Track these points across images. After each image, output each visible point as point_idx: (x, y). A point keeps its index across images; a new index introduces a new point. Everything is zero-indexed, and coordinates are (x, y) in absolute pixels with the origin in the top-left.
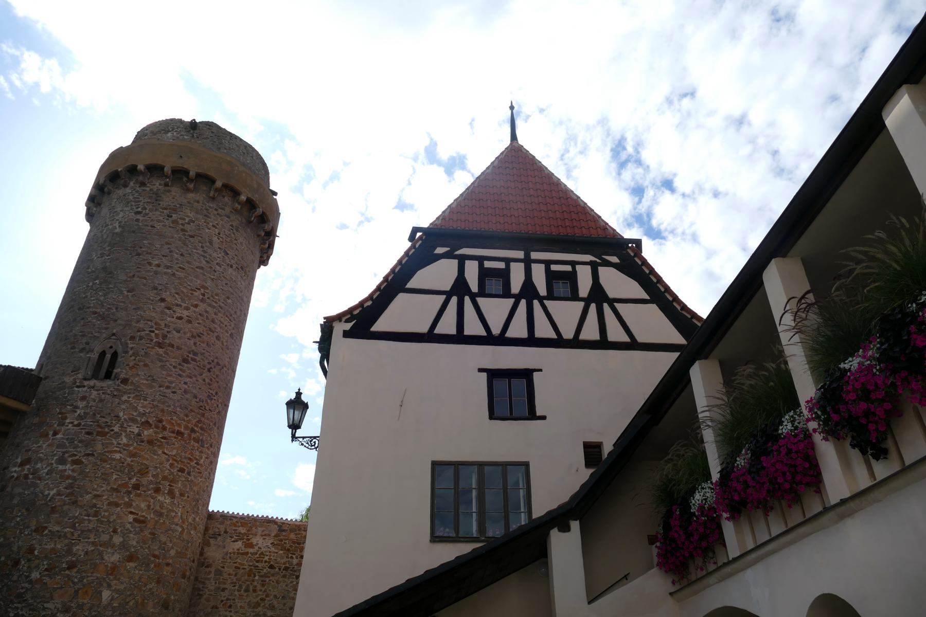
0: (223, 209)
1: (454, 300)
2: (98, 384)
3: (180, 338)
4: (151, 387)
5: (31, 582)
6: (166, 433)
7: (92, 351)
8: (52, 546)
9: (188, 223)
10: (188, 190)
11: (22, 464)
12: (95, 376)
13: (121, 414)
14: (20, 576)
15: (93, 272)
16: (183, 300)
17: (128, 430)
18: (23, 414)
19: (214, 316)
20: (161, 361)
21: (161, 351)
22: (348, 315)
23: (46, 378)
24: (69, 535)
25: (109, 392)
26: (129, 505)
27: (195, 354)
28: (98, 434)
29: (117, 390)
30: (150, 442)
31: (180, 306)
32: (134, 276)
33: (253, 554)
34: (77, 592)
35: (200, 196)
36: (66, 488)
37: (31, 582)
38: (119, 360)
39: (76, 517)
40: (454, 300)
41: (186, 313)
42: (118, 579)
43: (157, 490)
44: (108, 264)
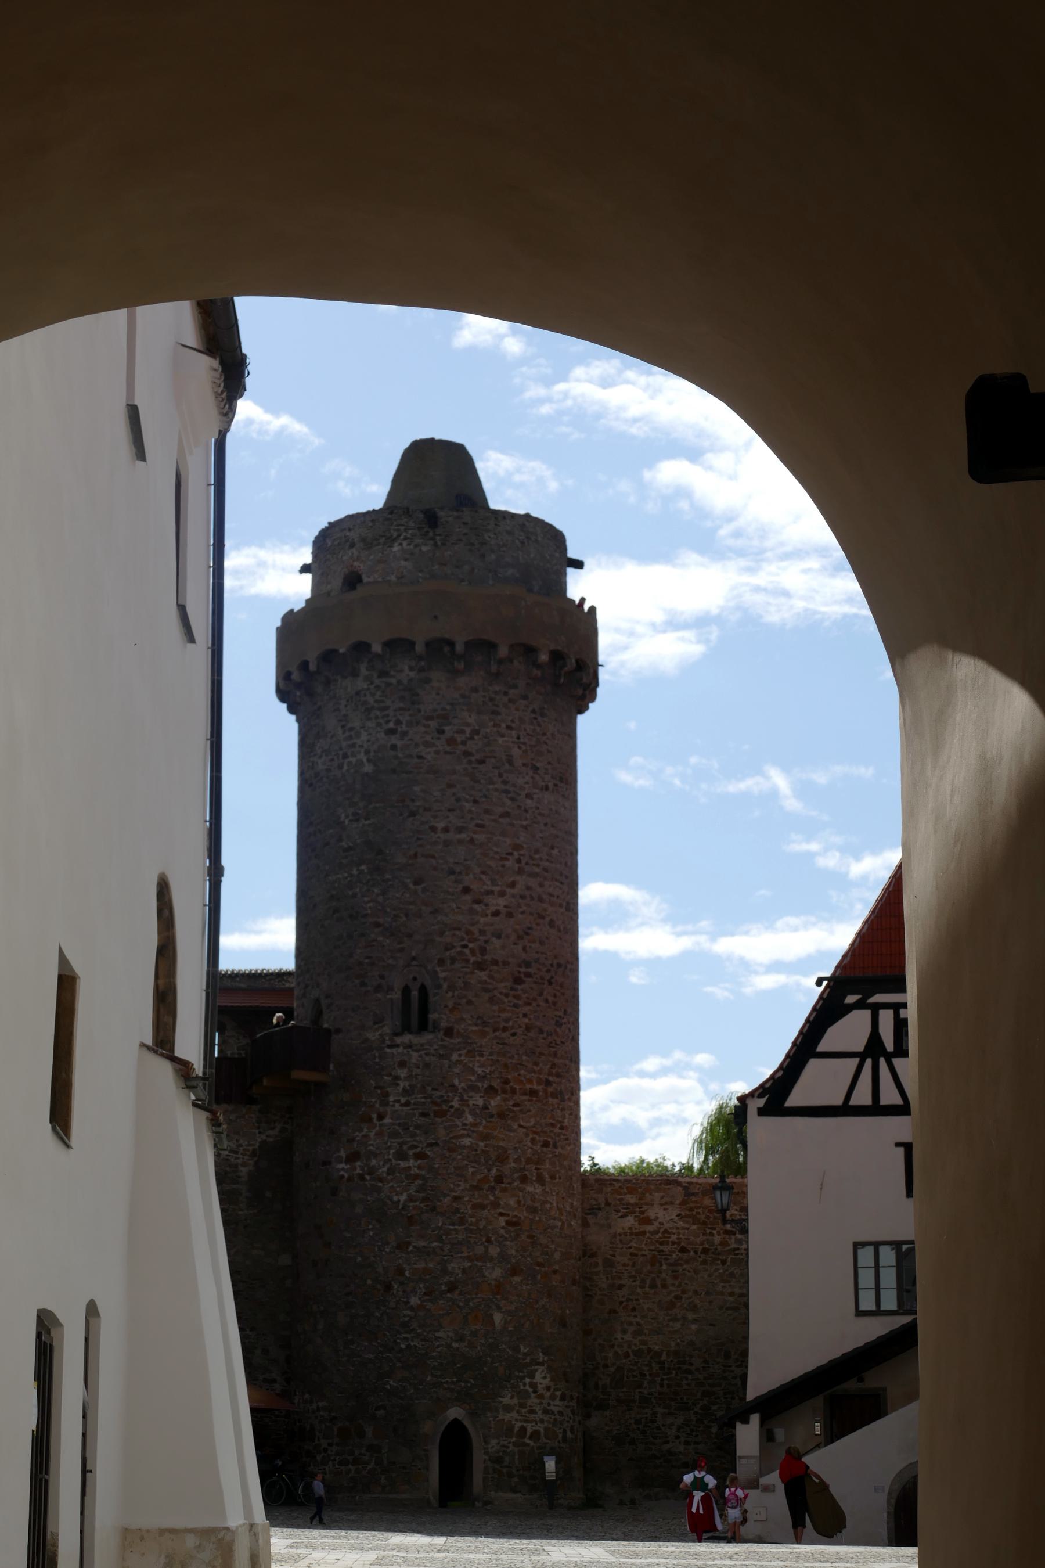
0: (515, 687)
1: (869, 1062)
2: (416, 1040)
3: (503, 947)
4: (483, 1034)
5: (412, 1308)
6: (518, 1098)
7: (390, 989)
8: (423, 1265)
9: (471, 738)
12: (406, 1028)
13: (456, 1082)
15: (350, 849)
16: (494, 882)
17: (471, 1103)
20: (486, 990)
21: (483, 975)
22: (762, 1090)
23: (338, 1031)
25: (432, 1051)
26: (496, 1205)
27: (528, 965)
28: (437, 1114)
30: (501, 1115)
31: (492, 892)
32: (416, 855)
36: (417, 1191)
38: (432, 999)
40: (869, 1062)
41: (502, 902)
43: (524, 1179)
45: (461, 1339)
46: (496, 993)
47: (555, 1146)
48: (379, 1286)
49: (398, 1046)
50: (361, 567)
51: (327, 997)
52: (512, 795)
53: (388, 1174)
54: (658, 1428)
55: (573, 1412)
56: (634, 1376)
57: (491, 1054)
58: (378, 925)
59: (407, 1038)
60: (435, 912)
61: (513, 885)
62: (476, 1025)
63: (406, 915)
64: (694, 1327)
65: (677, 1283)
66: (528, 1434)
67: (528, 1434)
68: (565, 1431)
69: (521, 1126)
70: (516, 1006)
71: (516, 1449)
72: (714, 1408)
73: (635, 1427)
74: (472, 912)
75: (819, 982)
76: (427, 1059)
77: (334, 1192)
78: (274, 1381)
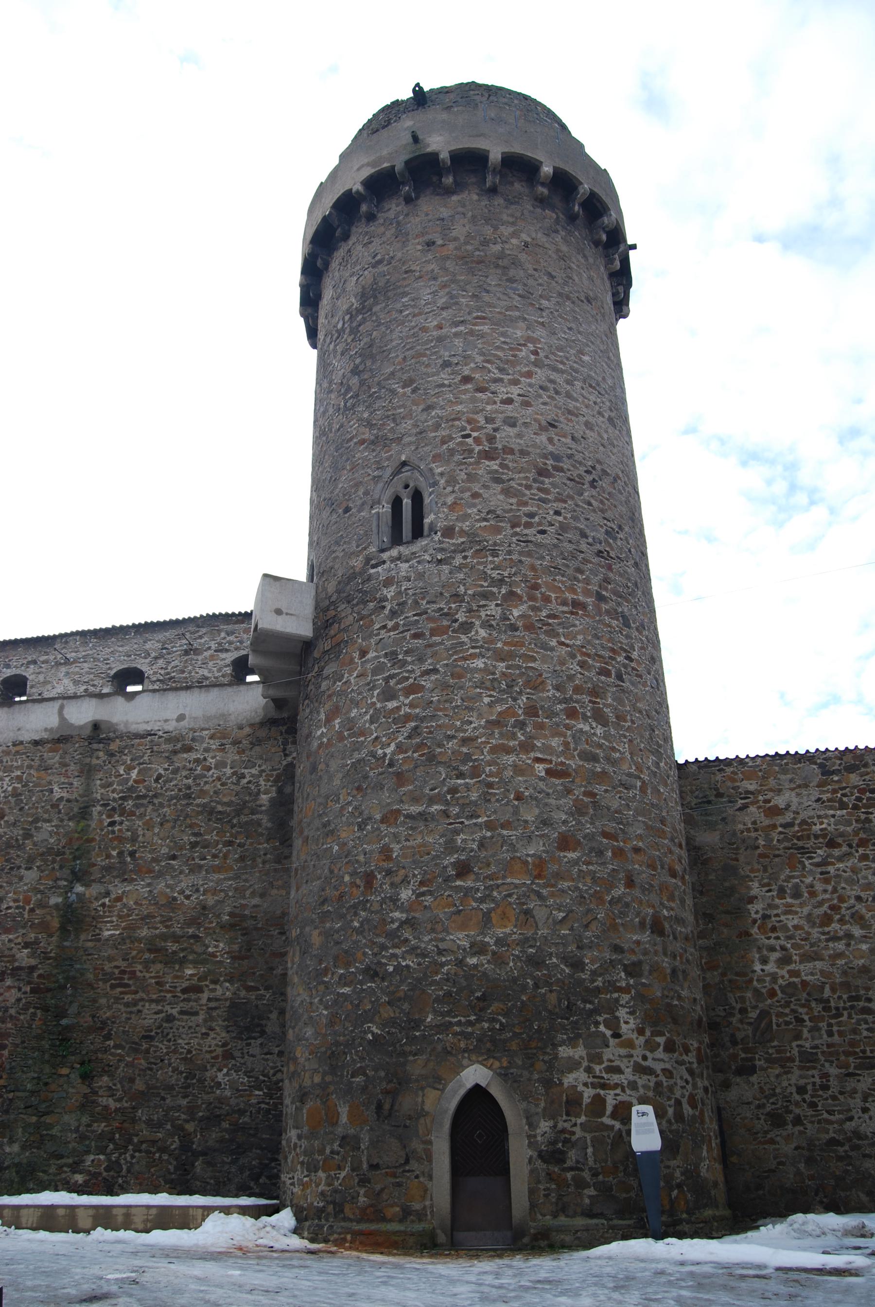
3: (519, 436)
4: (498, 530)
8: (419, 840)
10: (449, 192)
11: (329, 720)
12: (397, 539)
16: (501, 370)
19: (569, 387)
20: (498, 480)
21: (494, 465)
25: (428, 558)
27: (557, 458)
29: (442, 550)
31: (501, 380)
32: (405, 359)
33: (785, 826)
38: (427, 501)
41: (515, 391)
43: (572, 713)
46: (512, 483)
49: (384, 562)
53: (372, 722)
54: (834, 1098)
55: (691, 1072)
56: (787, 1023)
60: (429, 408)
61: (529, 375)
62: (485, 520)
63: (394, 420)
65: (830, 888)
66: (609, 1109)
67: (609, 1109)
68: (678, 1103)
69: (563, 644)
70: (544, 501)
71: (589, 1137)
73: (798, 1098)
74: (473, 400)
76: (420, 567)
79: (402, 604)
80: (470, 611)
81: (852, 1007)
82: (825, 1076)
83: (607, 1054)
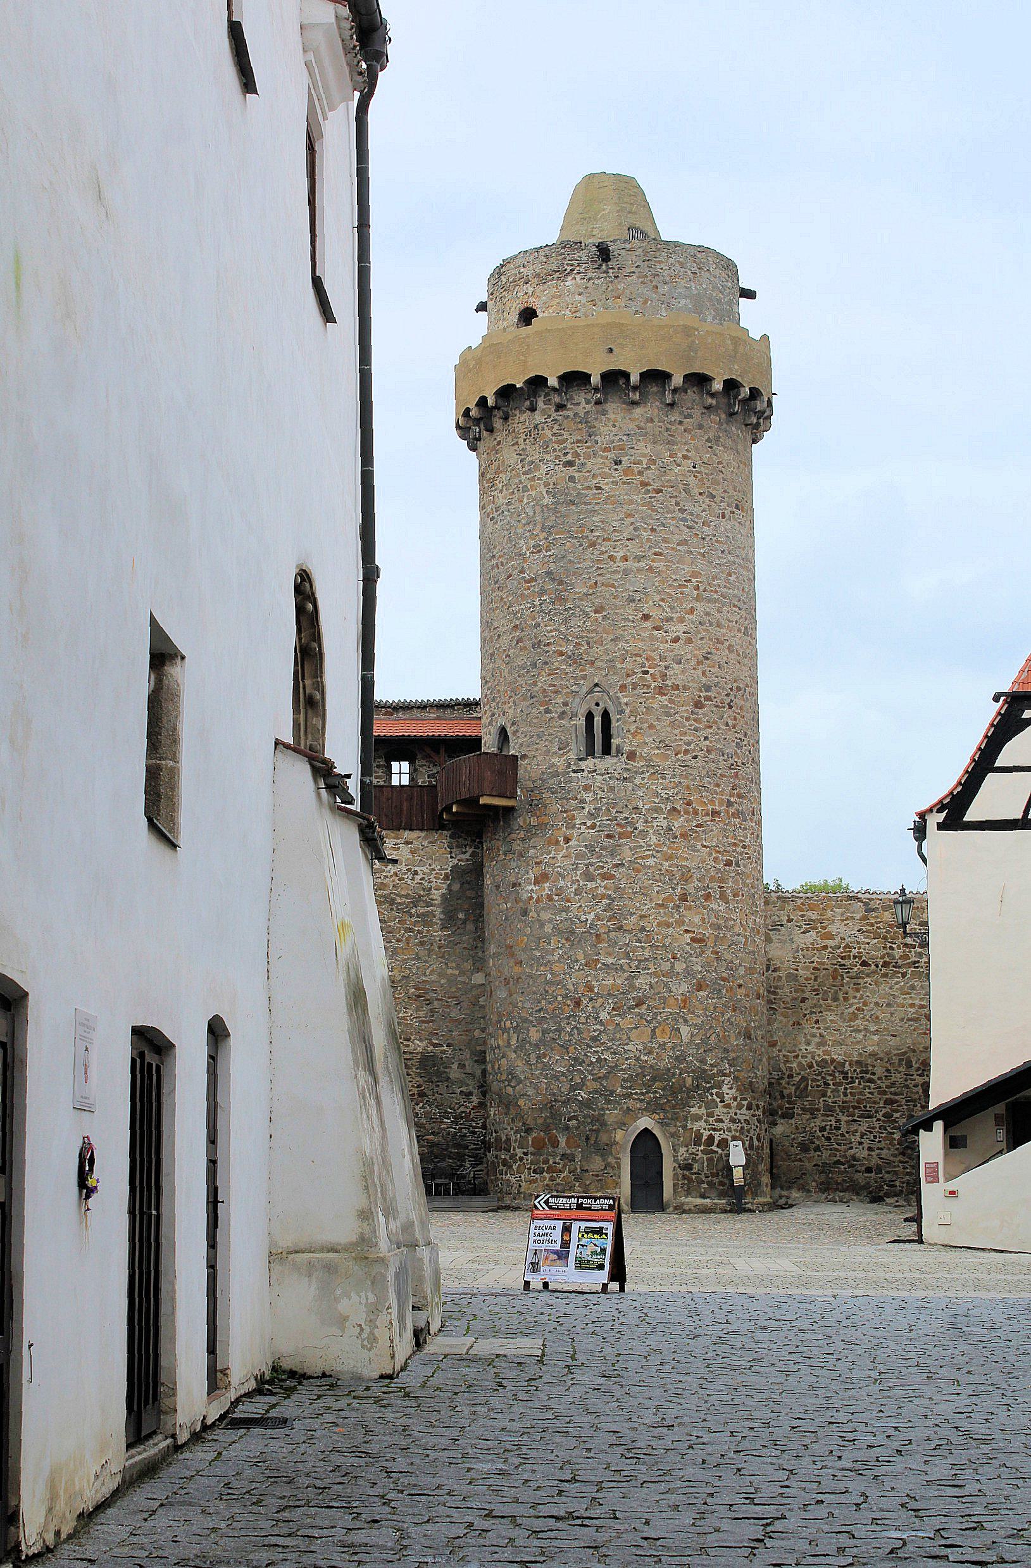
0: (690, 416)
3: (683, 672)
4: (666, 757)
5: (601, 1023)
6: (701, 819)
7: (574, 715)
9: (648, 468)
12: (590, 752)
13: (640, 805)
14: (587, 1018)
15: (532, 580)
16: (672, 608)
18: (511, 809)
19: (718, 616)
20: (668, 714)
21: (664, 699)
22: (941, 807)
23: (524, 757)
24: (626, 967)
34: (653, 1031)
35: (651, 409)
37: (601, 1023)
38: (614, 724)
39: (628, 945)
41: (682, 628)
42: (693, 1013)
43: (708, 897)
44: (552, 566)
45: (650, 1053)
47: (737, 865)
48: (569, 1002)
50: (533, 302)
51: (513, 724)
52: (689, 523)
53: (576, 894)
54: (842, 1135)
56: (818, 1086)
57: (673, 776)
58: (561, 654)
59: (590, 763)
61: (692, 611)
62: (658, 748)
63: (588, 644)
64: (876, 1038)
66: (716, 1142)
67: (716, 1142)
68: (751, 1138)
70: (696, 730)
72: (896, 1115)
74: (651, 636)
75: (996, 698)
77: (525, 913)
78: (471, 1094)
79: (597, 809)
80: (646, 822)
81: (862, 1078)
82: (838, 1121)
83: (717, 1112)
